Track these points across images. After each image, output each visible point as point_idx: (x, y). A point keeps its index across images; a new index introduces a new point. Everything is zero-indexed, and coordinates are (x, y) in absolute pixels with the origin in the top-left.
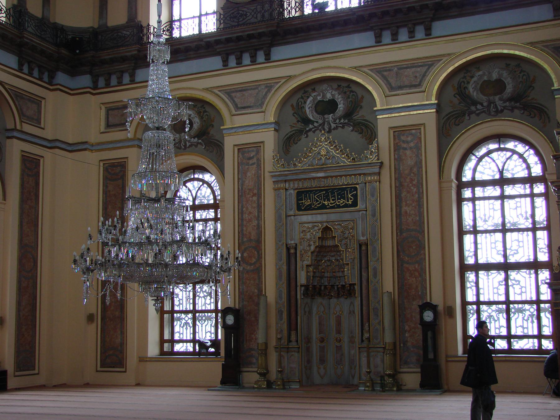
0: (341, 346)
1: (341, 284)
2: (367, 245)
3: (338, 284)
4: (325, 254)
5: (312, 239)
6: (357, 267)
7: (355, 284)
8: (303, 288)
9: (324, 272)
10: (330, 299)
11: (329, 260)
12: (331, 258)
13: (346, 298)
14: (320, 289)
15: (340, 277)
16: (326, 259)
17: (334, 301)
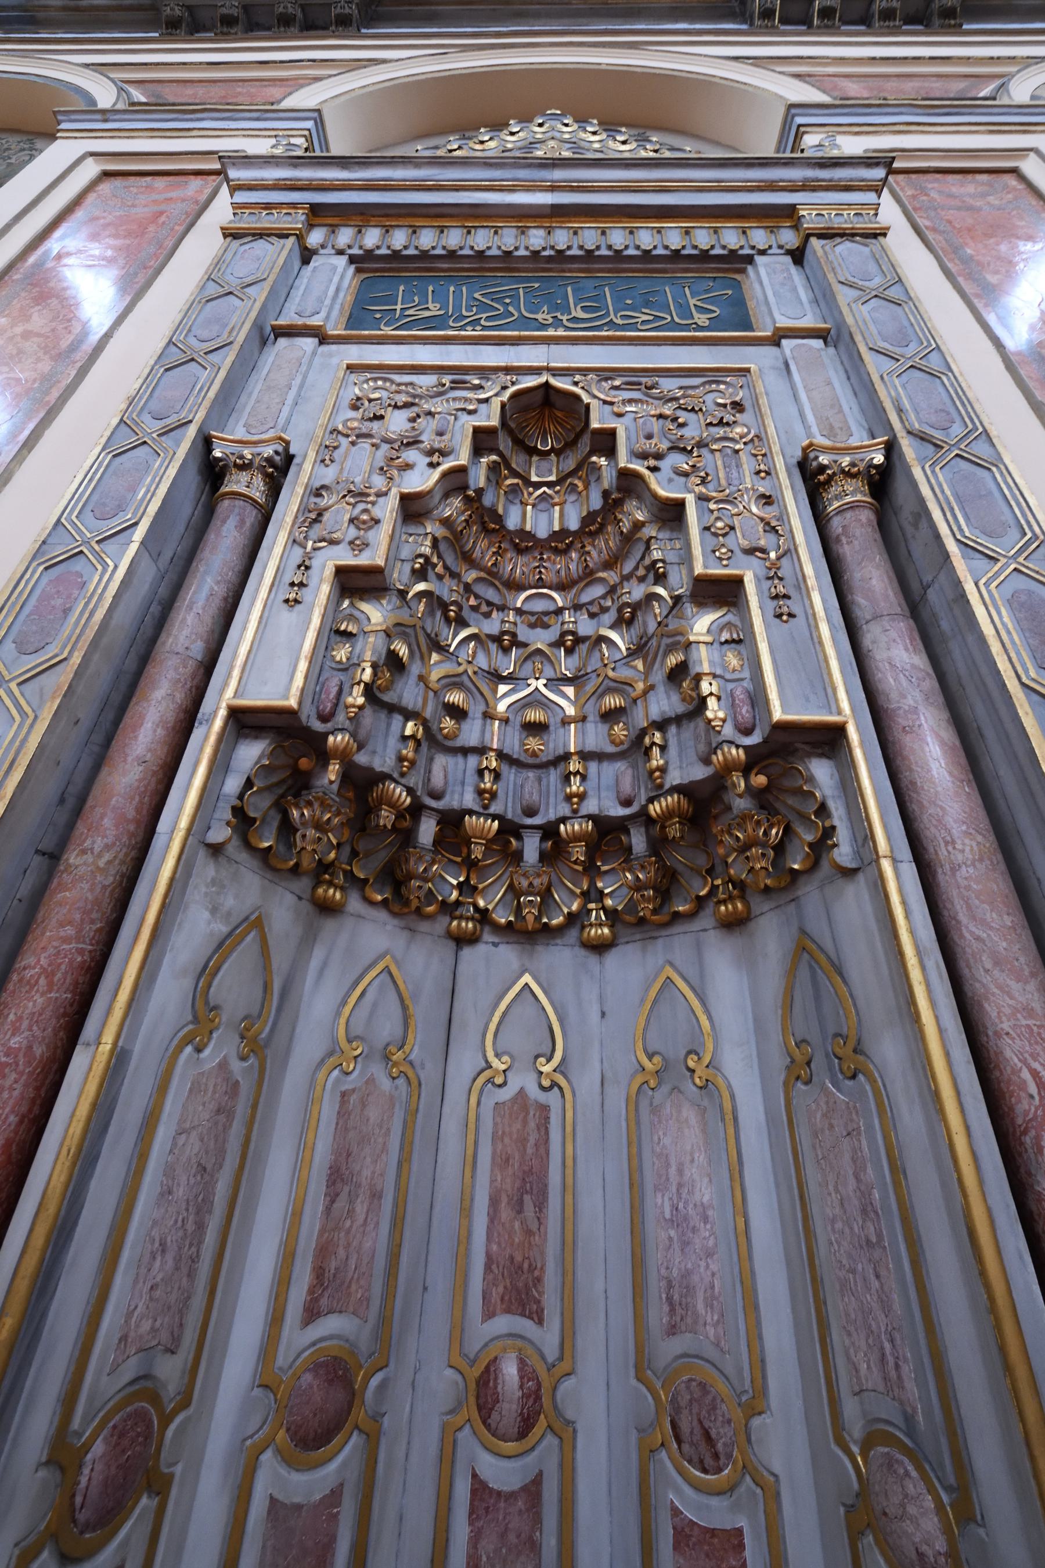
0: (533, 1490)
1: (591, 806)
2: (882, 482)
3: (553, 810)
4: (490, 594)
5: (428, 439)
6: (820, 600)
7: (830, 739)
8: (251, 753)
9: (458, 713)
10: (462, 941)
11: (505, 641)
12: (524, 633)
13: (600, 948)
14: (406, 836)
15: (585, 756)
16: (492, 626)
17: (490, 960)
